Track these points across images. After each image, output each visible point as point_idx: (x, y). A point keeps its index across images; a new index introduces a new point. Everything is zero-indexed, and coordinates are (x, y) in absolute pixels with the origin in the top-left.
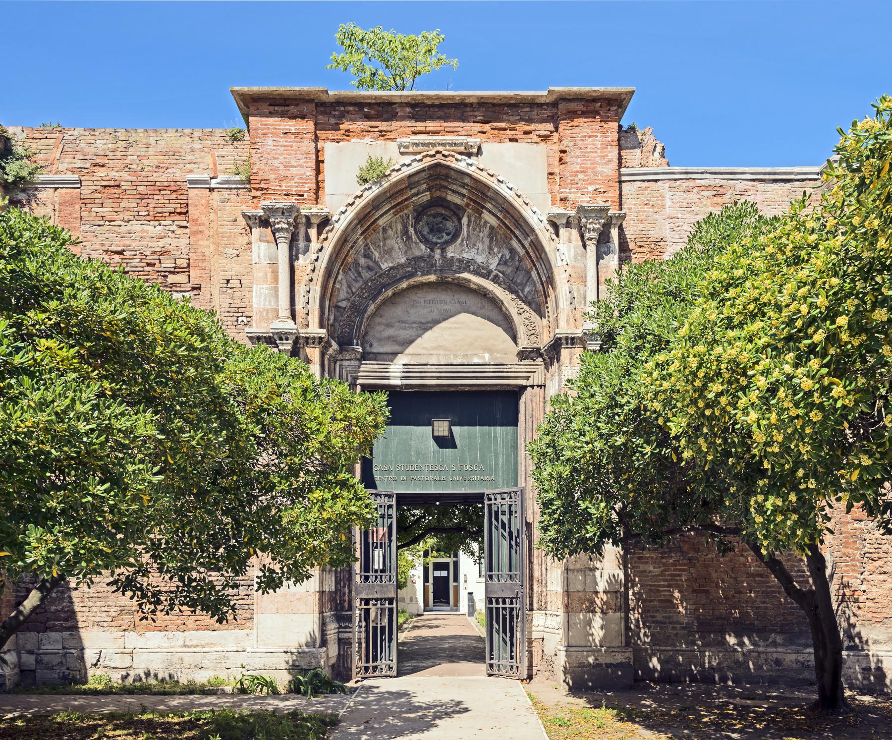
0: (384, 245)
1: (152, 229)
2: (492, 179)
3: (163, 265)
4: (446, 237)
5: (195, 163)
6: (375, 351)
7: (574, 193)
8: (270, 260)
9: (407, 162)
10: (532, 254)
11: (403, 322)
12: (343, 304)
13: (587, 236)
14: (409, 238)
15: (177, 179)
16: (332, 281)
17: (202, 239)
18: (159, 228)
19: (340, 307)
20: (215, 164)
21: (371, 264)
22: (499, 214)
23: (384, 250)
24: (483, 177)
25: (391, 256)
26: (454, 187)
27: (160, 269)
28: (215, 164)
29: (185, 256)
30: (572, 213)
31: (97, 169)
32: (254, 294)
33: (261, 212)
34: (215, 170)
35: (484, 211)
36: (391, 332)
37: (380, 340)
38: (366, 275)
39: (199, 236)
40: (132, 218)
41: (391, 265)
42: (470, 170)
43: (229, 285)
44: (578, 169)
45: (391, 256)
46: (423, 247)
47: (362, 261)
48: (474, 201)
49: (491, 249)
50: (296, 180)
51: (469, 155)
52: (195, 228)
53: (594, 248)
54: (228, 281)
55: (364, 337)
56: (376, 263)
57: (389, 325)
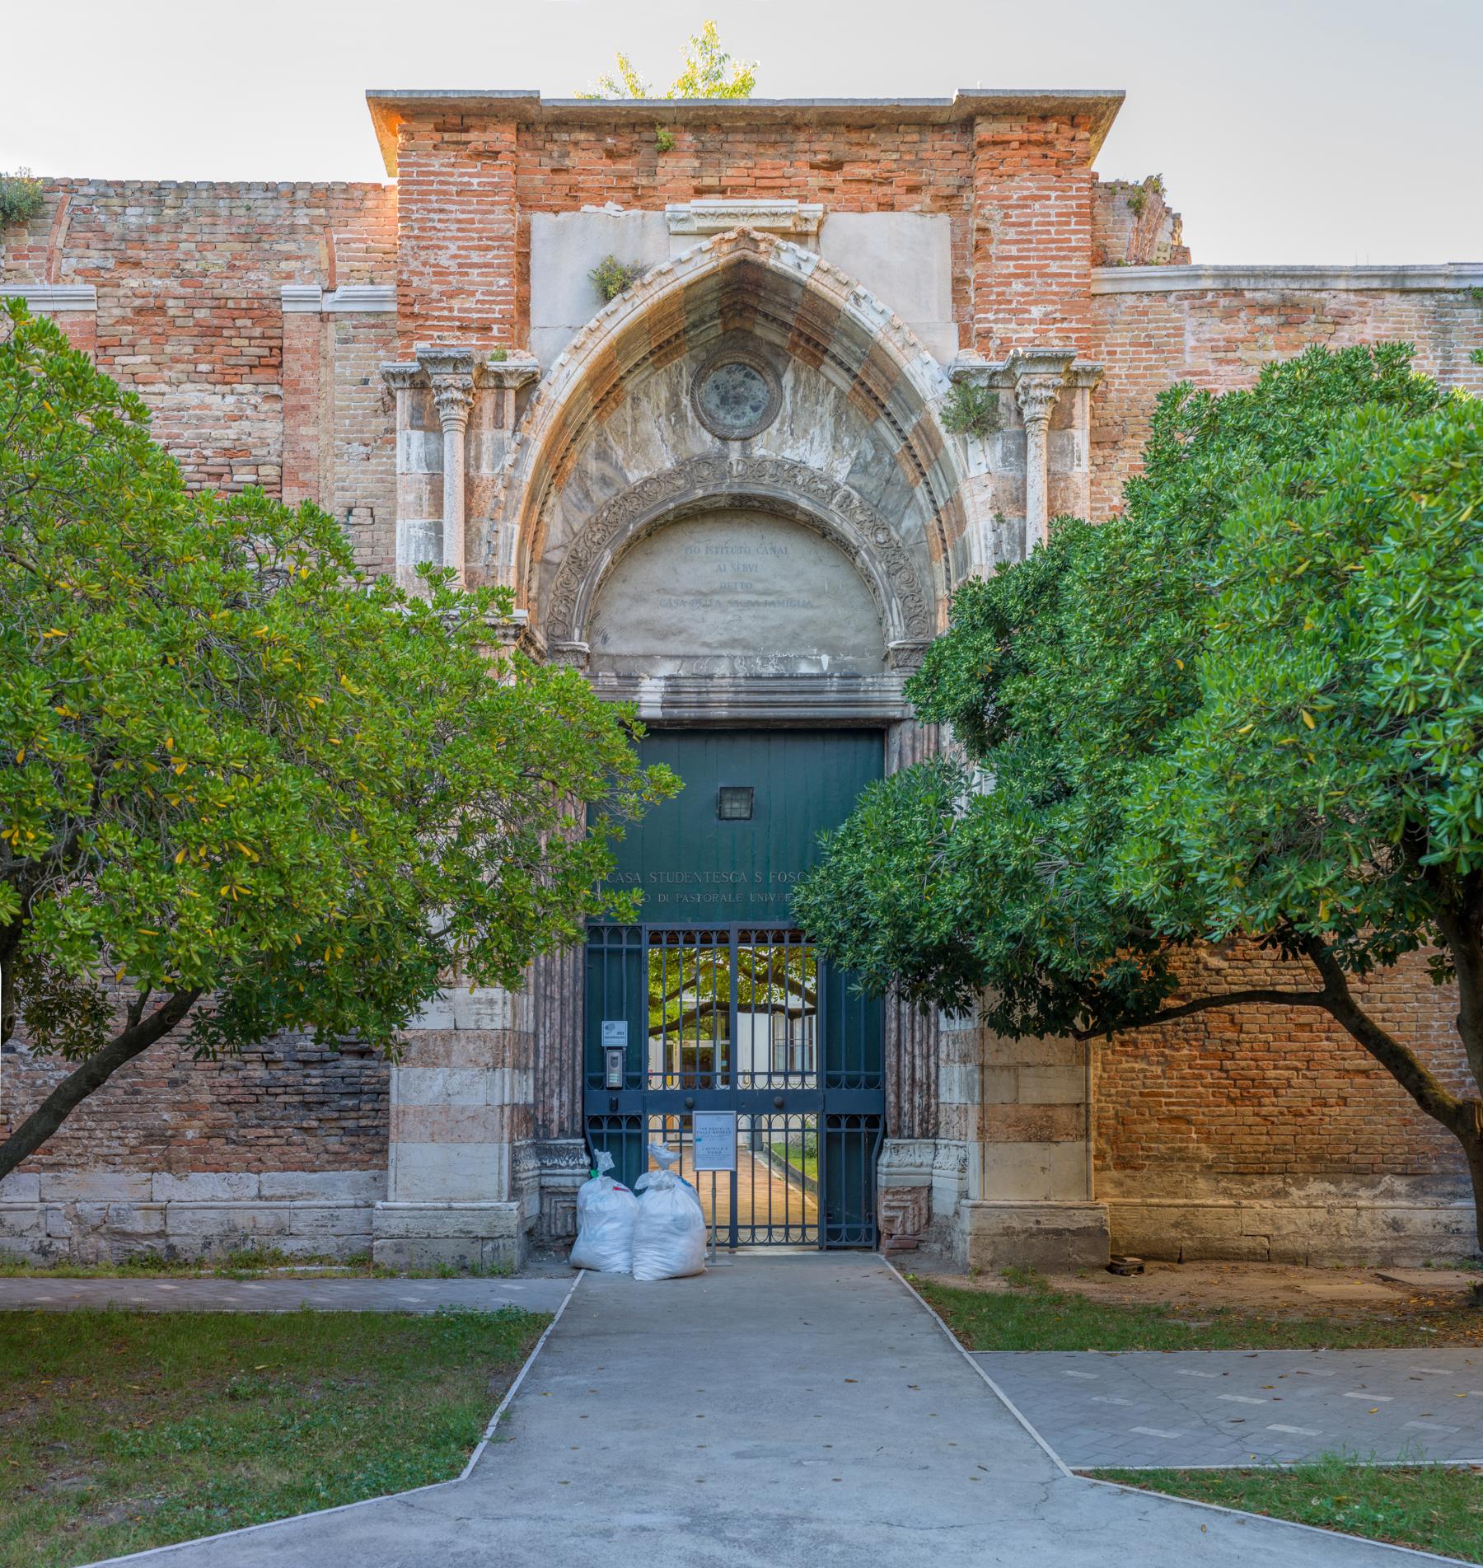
0: (634, 432)
1: (221, 402)
2: (845, 292)
3: (236, 478)
4: (751, 415)
5: (298, 258)
6: (612, 650)
7: (1004, 321)
8: (428, 466)
9: (685, 254)
10: (918, 451)
11: (665, 591)
12: (556, 556)
13: (1027, 412)
14: (682, 418)
15: (265, 292)
16: (537, 508)
17: (305, 424)
18: (230, 399)
19: (548, 562)
20: (332, 261)
21: (609, 472)
22: (854, 367)
23: (635, 443)
24: (825, 288)
25: (645, 455)
26: (770, 309)
27: (231, 486)
28: (332, 261)
29: (274, 459)
30: (999, 365)
31: (125, 271)
32: (398, 537)
33: (413, 366)
34: (332, 275)
35: (826, 359)
36: (642, 612)
37: (622, 628)
38: (600, 495)
39: (302, 416)
40: (183, 377)
41: (646, 474)
42: (805, 274)
43: (352, 520)
44: (1012, 270)
45: (645, 455)
46: (707, 437)
47: (593, 466)
48: (808, 340)
49: (836, 439)
50: (478, 296)
51: (801, 237)
52: (292, 400)
53: (1042, 440)
54: (350, 512)
55: (591, 623)
56: (618, 469)
57: (639, 599)
